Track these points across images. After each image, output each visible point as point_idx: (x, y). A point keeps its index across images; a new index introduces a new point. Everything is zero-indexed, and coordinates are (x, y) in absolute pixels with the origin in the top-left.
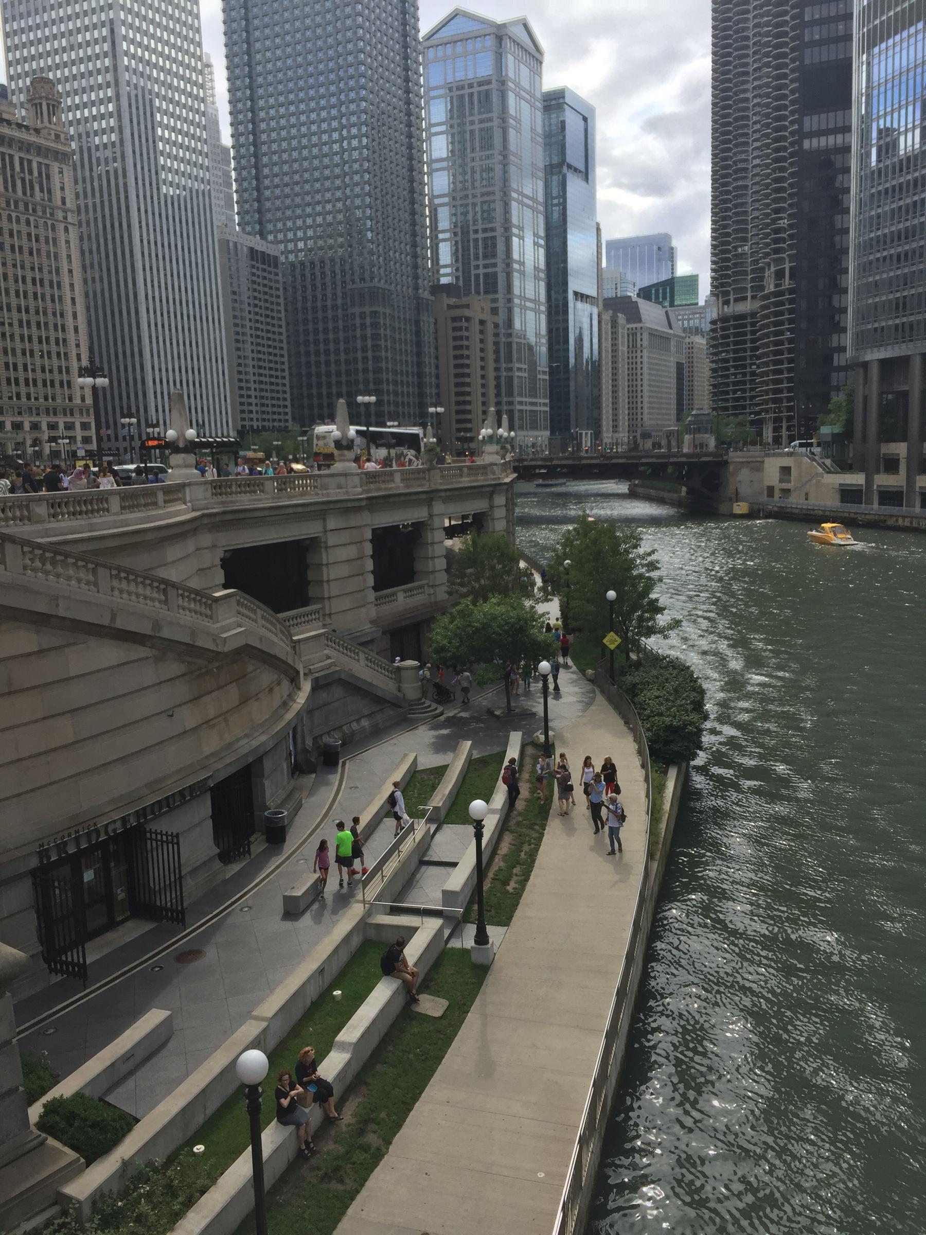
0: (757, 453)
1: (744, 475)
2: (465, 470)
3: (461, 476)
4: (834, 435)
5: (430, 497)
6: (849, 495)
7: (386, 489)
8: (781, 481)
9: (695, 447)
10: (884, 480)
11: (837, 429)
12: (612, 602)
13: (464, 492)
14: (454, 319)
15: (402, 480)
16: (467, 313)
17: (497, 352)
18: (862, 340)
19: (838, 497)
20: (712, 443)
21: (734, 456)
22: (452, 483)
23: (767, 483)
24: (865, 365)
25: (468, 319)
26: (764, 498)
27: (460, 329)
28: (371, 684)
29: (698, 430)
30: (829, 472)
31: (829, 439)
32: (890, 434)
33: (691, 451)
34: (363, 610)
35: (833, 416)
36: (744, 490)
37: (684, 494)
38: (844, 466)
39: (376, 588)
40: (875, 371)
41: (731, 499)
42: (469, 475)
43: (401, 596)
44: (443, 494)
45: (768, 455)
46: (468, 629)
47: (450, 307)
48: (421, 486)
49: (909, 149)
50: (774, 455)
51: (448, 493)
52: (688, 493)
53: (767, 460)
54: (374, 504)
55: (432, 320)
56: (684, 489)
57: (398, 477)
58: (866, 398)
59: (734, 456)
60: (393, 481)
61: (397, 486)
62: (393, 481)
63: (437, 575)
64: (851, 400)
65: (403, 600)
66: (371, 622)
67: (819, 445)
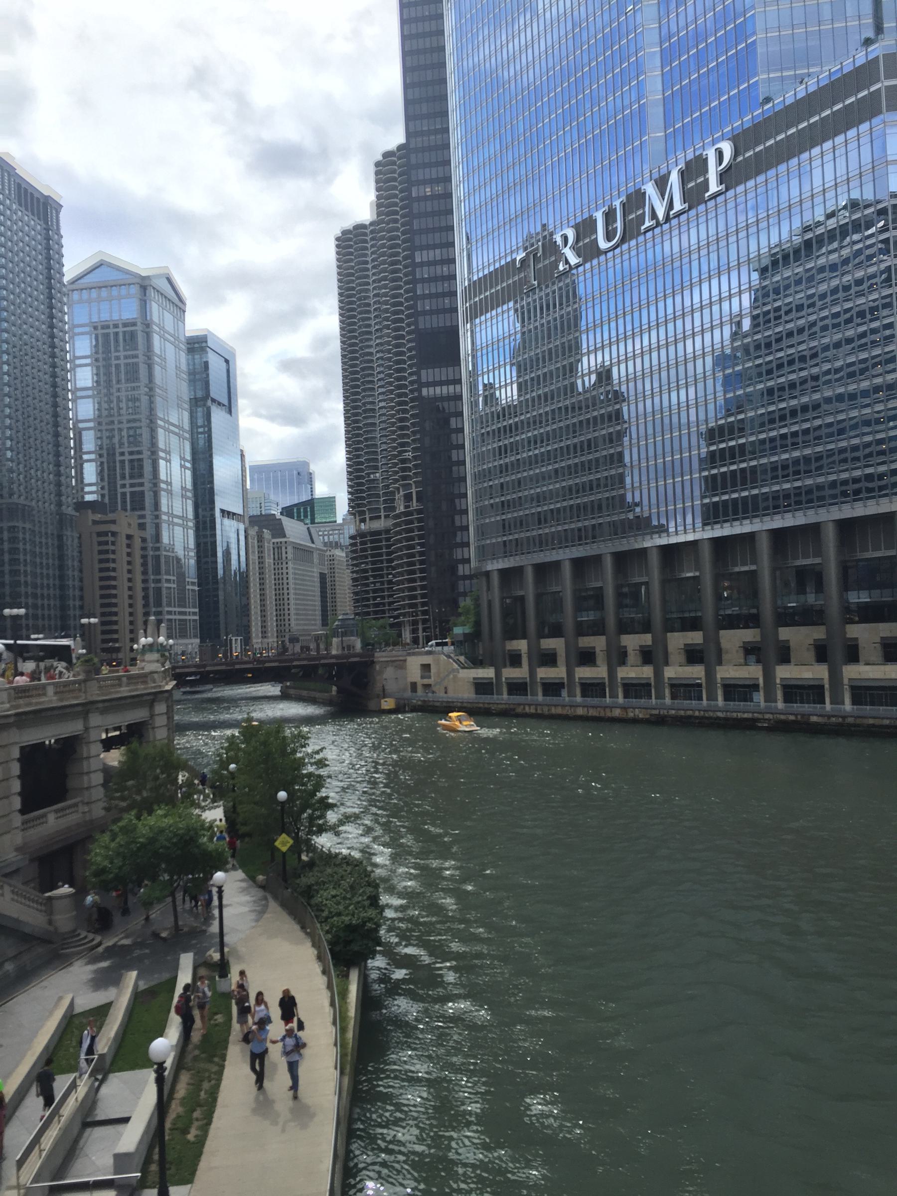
0: (400, 653)
2: (124, 679)
3: (120, 685)
4: (465, 635)
5: (85, 710)
6: (482, 687)
7: (37, 704)
8: (422, 677)
9: (343, 648)
10: (510, 673)
11: (467, 629)
12: (283, 803)
13: (123, 702)
14: (99, 534)
15: (56, 693)
16: (113, 528)
17: (144, 564)
18: (484, 553)
19: (473, 690)
20: (358, 645)
21: (381, 656)
22: (110, 693)
23: (411, 679)
24: (487, 574)
25: (114, 534)
26: (408, 694)
27: (107, 543)
28: (17, 921)
29: (344, 634)
31: (461, 638)
32: (512, 633)
33: (340, 652)
34: (8, 836)
35: (463, 618)
36: (391, 687)
37: (334, 693)
38: (476, 662)
39: (23, 812)
40: (495, 580)
41: (378, 696)
42: (128, 684)
43: (51, 818)
44: (100, 705)
45: (409, 654)
46: (133, 846)
47: (95, 522)
48: (76, 698)
49: (718, 346)
50: (414, 654)
51: (106, 704)
52: (338, 692)
53: (409, 659)
54: (23, 720)
55: (76, 535)
56: (334, 688)
57: (50, 690)
60: (45, 694)
61: (50, 699)
62: (45, 694)
63: (93, 791)
64: (478, 605)
65: (53, 822)
66: (18, 849)
67: (453, 644)
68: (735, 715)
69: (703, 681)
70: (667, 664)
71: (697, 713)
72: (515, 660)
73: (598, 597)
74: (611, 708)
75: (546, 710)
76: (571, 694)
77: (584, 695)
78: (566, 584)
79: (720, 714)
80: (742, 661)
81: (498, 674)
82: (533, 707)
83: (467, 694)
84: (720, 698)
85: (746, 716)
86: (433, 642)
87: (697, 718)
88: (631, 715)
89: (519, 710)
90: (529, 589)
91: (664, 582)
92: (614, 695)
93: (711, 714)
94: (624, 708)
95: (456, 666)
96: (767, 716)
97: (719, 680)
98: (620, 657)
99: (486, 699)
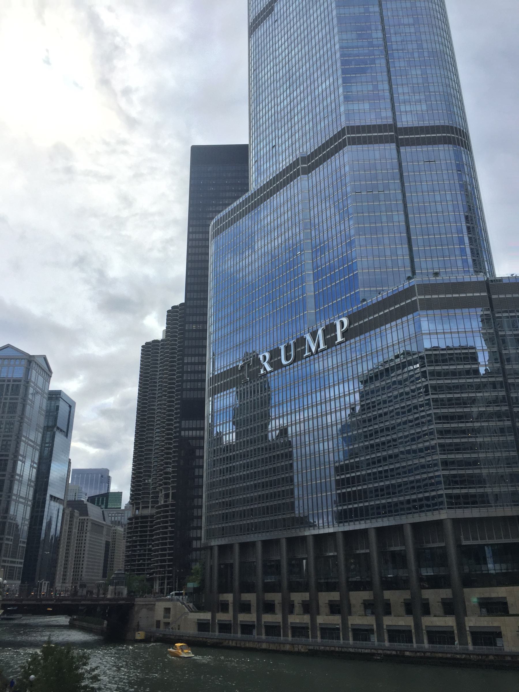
1: (144, 613)
4: (194, 589)
6: (202, 626)
8: (165, 617)
10: (221, 617)
18: (210, 534)
19: (196, 627)
20: (125, 592)
21: (139, 601)
24: (211, 548)
30: (192, 612)
32: (224, 588)
35: (194, 577)
38: (200, 608)
45: (158, 601)
53: (157, 603)
58: (211, 567)
59: (139, 601)
67: (186, 594)
68: (360, 650)
69: (340, 626)
70: (318, 614)
71: (337, 649)
72: (224, 607)
73: (278, 565)
74: (284, 644)
75: (242, 645)
76: (259, 634)
77: (267, 634)
78: (258, 557)
79: (351, 650)
80: (363, 613)
81: (213, 617)
82: (234, 642)
83: (192, 631)
84: (351, 638)
85: (366, 651)
86: (174, 592)
87: (337, 652)
88: (296, 649)
89: (225, 643)
90: (236, 559)
91: (316, 558)
92: (286, 635)
93: (345, 650)
94: (292, 644)
95: (187, 610)
96: (380, 652)
97: (350, 626)
98: (289, 608)
99: (205, 634)
